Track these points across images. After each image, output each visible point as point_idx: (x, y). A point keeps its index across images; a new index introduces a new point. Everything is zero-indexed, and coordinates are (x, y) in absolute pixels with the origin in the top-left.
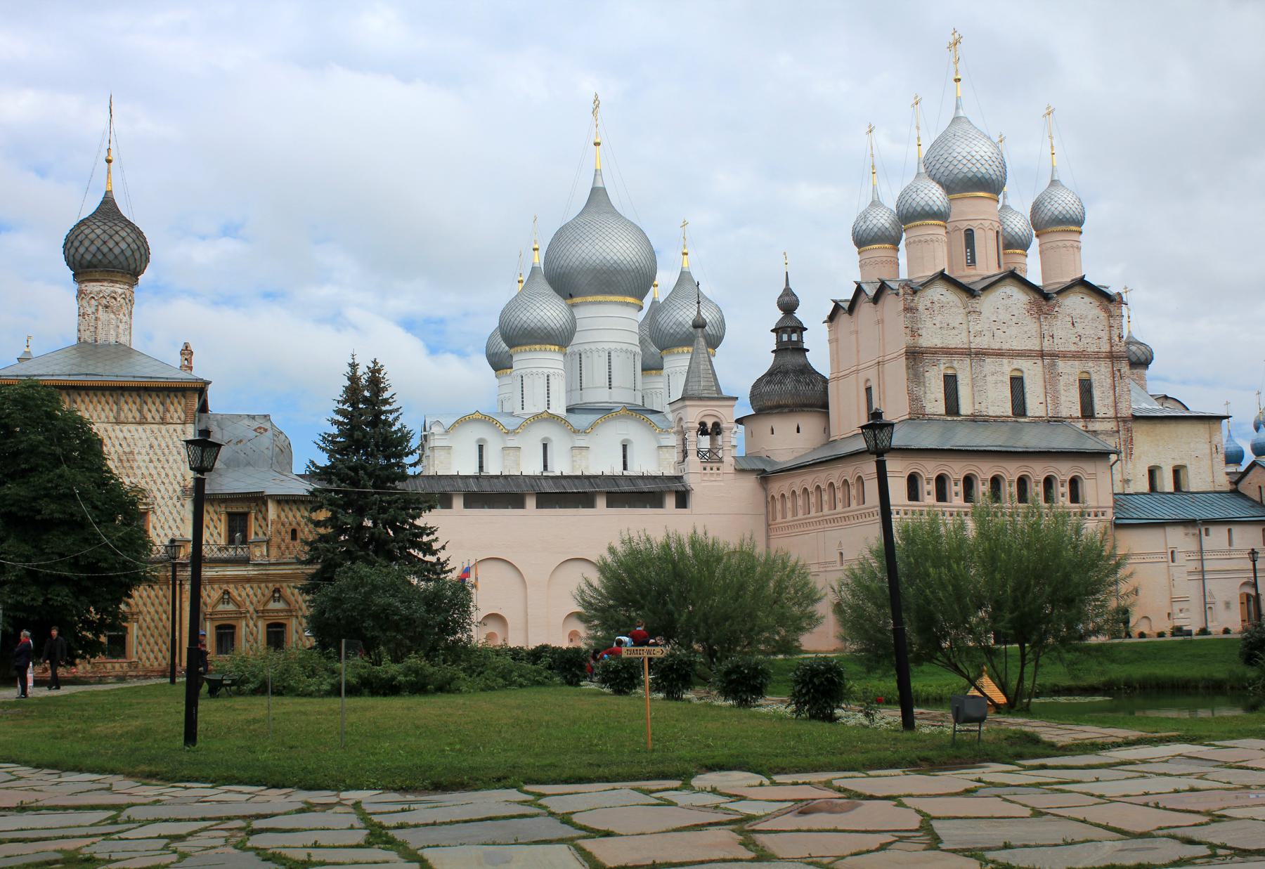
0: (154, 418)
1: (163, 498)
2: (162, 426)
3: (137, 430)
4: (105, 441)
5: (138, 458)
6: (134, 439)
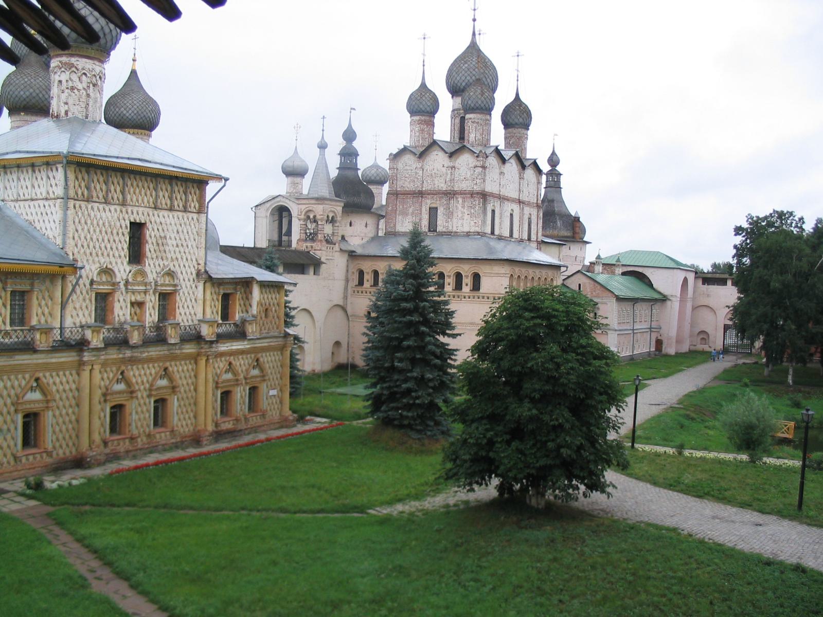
0: (179, 206)
1: (184, 280)
2: (184, 214)
3: (169, 216)
4: (148, 225)
5: (169, 242)
6: (167, 225)
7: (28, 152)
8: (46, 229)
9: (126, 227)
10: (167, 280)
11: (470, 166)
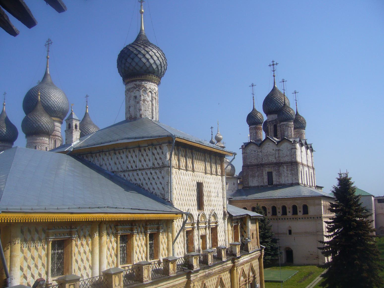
7: (128, 139)
8: (154, 189)
9: (195, 185)
10: (212, 219)
11: (289, 148)
